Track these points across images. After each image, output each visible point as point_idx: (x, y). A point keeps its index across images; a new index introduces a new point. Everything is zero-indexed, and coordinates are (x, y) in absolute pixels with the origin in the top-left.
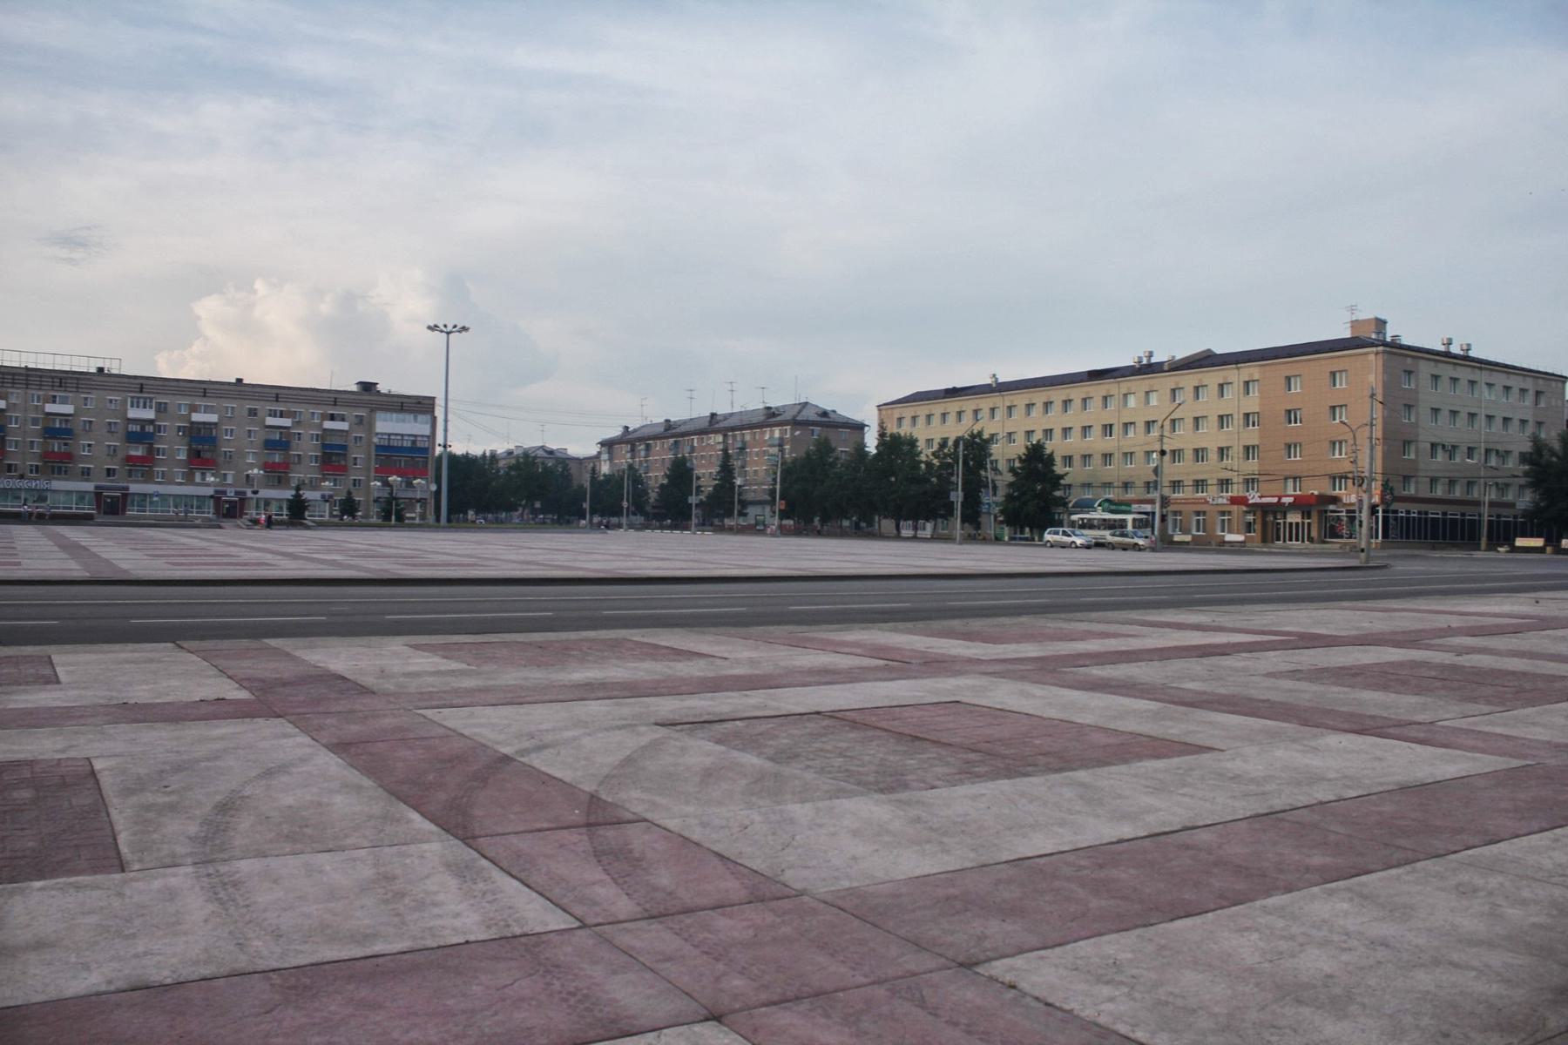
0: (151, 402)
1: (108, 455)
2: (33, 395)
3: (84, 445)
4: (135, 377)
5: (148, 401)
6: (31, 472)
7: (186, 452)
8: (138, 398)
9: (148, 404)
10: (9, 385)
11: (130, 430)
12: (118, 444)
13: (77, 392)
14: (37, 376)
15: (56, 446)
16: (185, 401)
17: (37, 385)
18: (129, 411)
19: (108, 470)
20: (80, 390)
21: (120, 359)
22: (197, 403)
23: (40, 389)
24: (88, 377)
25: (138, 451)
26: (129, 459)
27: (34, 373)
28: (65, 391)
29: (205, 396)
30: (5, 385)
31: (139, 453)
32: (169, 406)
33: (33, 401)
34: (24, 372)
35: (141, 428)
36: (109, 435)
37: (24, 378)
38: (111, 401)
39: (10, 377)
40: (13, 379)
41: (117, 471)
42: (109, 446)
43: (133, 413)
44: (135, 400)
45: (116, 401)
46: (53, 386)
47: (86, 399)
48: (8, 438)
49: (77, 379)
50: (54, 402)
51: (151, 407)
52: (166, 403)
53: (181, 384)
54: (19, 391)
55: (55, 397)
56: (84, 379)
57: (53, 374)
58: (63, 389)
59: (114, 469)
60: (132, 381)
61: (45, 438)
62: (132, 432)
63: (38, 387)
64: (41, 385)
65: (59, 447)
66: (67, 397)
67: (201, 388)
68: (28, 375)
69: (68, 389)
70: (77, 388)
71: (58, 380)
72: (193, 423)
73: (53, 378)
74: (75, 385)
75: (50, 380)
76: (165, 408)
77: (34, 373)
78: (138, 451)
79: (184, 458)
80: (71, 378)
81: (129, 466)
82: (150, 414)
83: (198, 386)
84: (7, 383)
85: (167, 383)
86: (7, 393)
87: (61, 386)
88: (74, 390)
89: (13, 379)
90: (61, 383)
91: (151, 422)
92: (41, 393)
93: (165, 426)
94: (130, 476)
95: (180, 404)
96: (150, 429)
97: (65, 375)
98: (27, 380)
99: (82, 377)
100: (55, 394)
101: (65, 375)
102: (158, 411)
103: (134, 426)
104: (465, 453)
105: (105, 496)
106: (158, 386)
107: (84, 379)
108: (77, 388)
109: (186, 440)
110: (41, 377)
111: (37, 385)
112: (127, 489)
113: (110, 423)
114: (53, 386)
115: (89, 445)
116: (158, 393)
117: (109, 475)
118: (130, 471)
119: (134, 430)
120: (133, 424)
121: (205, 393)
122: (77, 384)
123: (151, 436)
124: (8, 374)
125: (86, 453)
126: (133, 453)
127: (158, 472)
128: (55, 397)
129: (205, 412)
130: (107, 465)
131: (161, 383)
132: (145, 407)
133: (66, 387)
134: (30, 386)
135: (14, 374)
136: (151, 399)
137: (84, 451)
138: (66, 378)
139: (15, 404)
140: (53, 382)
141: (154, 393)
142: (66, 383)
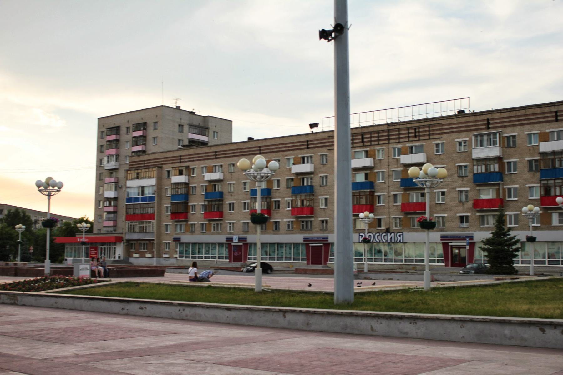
0: (495, 137)
1: (460, 202)
2: (394, 149)
3: (438, 193)
4: (481, 113)
5: (492, 137)
6: (396, 226)
7: (539, 189)
8: (482, 135)
9: (485, 142)
10: (376, 143)
11: (475, 172)
12: (469, 189)
13: (429, 139)
14: (394, 130)
15: (414, 198)
16: (537, 129)
17: (396, 139)
18: (473, 151)
19: (462, 217)
20: (432, 137)
21: (469, 98)
22: (548, 131)
23: (399, 142)
24: (438, 122)
25: (488, 194)
26: (478, 204)
27: (393, 127)
28: (419, 140)
29: (557, 120)
30: (373, 143)
31: (490, 197)
32: (517, 137)
33: (395, 156)
34: (385, 128)
35: (486, 169)
36: (461, 179)
37: (386, 134)
38: (460, 143)
39: (376, 135)
40: (378, 137)
41: (470, 219)
42: (461, 192)
43: (478, 153)
44: (479, 138)
45: (465, 142)
46: (409, 137)
47: (437, 145)
48: (376, 194)
49: (429, 126)
50: (412, 153)
51: (495, 143)
52: (514, 137)
53: (529, 112)
54: (384, 147)
55: (412, 147)
56: (435, 125)
57: (409, 126)
58: (417, 138)
59: (467, 217)
60: (478, 118)
61: (405, 190)
62: (478, 174)
63: (397, 141)
64: (399, 138)
65: (417, 198)
66: (422, 146)
67: (551, 112)
68: (389, 131)
69: (421, 138)
70: (429, 135)
71: (413, 131)
72: (541, 154)
73: (408, 129)
74: (428, 133)
75: (407, 132)
76: (514, 142)
77: (393, 127)
78: (488, 194)
79: (539, 198)
80: (424, 126)
81: (478, 211)
82: (494, 151)
83: (547, 109)
84: (375, 141)
85: (513, 114)
86: (374, 150)
87: (415, 136)
88: (427, 137)
89: (378, 137)
90: (415, 132)
91: (499, 159)
92: (400, 146)
93: (515, 163)
94: (483, 224)
95: (530, 135)
96: (495, 167)
97: (418, 124)
98: (388, 135)
99: (432, 123)
100: (411, 144)
101: (418, 124)
102: (502, 146)
103: (479, 167)
104: (323, 40)
105: (452, 248)
106: (504, 118)
107: (435, 125)
108: (429, 135)
109: (538, 175)
110: (399, 130)
111: (396, 139)
112: (471, 237)
113: (460, 167)
114: (409, 137)
115: (443, 193)
116: (505, 126)
117: (462, 222)
118: (483, 217)
119: (479, 171)
120: (478, 165)
121: (557, 116)
122: (429, 131)
123: (500, 175)
124: (375, 132)
125: (440, 202)
126: (484, 197)
127: (510, 216)
128: (412, 147)
129: (559, 139)
130: (459, 213)
131: (507, 114)
132: (481, 145)
133: (419, 136)
134: (391, 141)
135: (378, 132)
136: (495, 134)
137: (439, 200)
138: (419, 127)
139: (380, 160)
140: (409, 133)
141: (501, 127)
142: (419, 132)
